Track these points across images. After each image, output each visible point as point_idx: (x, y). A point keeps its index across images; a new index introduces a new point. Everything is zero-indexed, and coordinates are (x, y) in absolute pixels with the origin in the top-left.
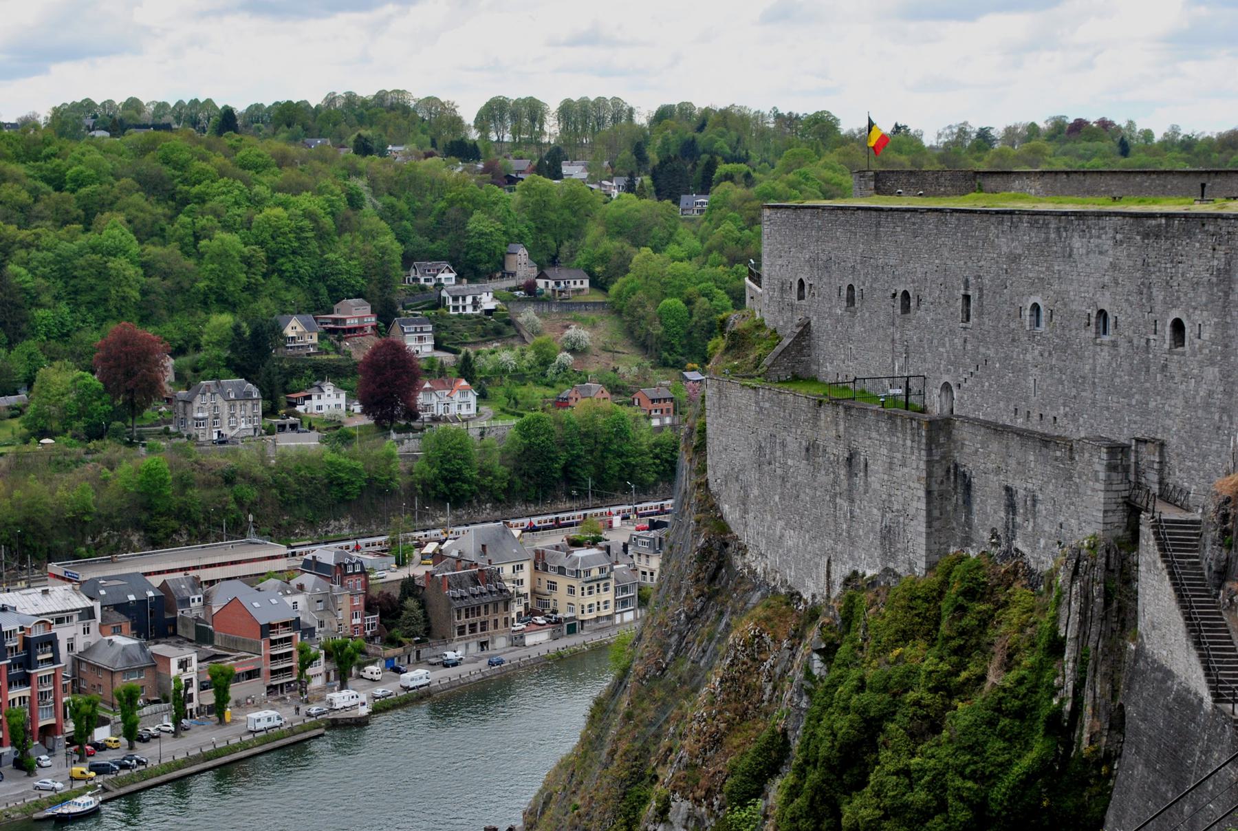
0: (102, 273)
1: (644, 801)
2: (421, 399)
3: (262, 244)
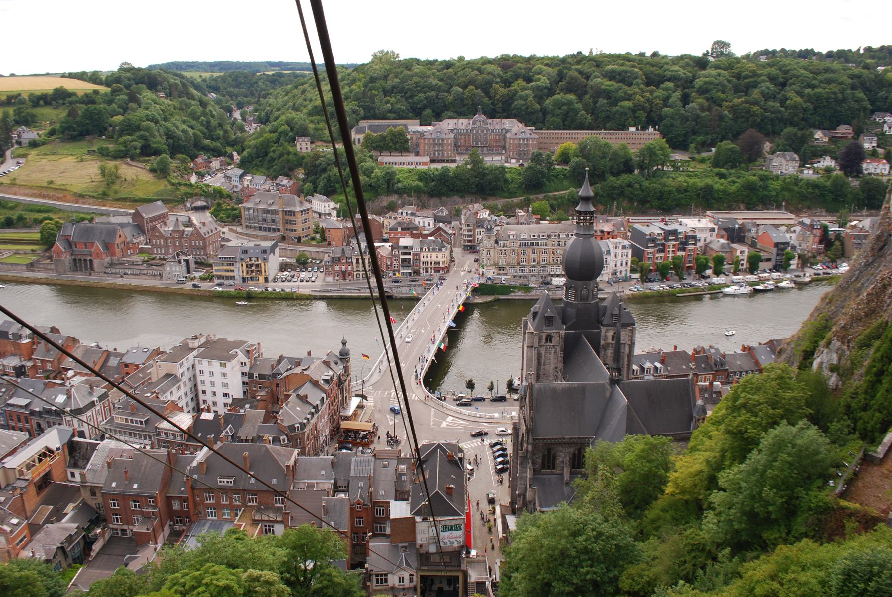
0: (748, 112)
1: (823, 338)
2: (864, 166)
3: (812, 103)
